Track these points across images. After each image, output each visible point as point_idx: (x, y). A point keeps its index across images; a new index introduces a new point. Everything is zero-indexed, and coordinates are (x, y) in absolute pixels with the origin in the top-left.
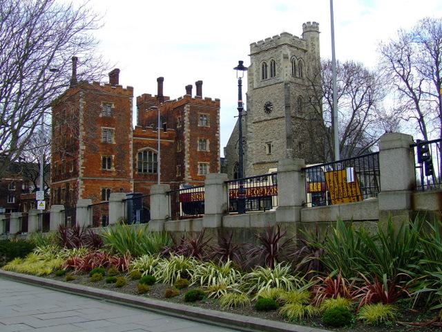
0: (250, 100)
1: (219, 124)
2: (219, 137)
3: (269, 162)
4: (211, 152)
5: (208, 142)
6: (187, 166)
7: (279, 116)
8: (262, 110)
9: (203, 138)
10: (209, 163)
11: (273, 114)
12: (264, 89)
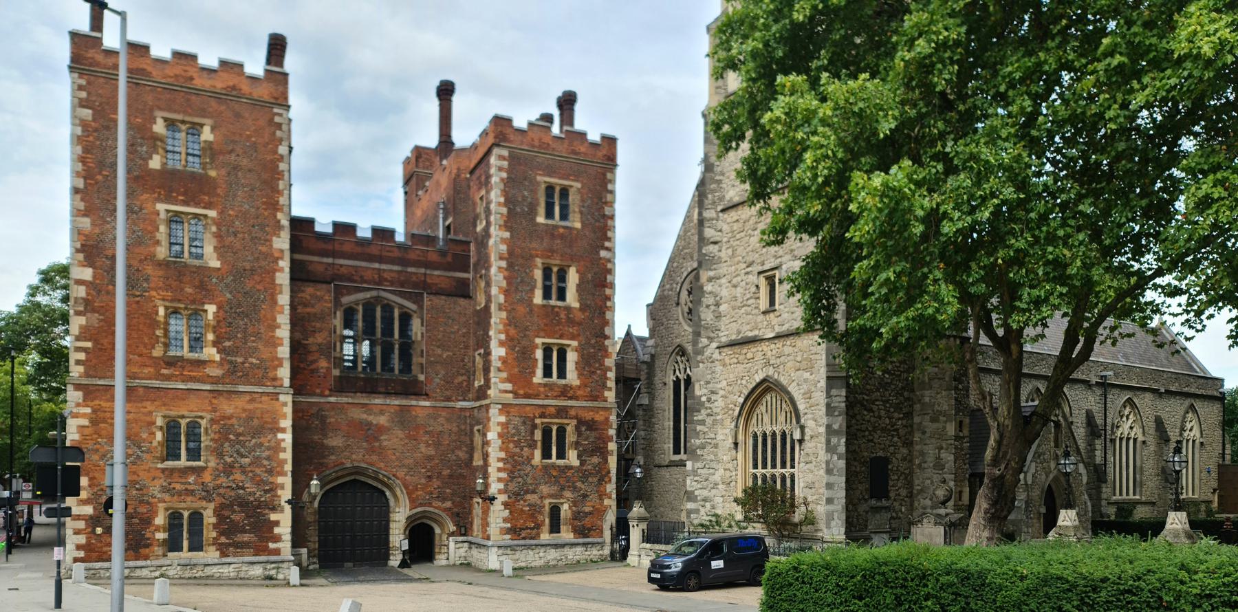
1: (612, 217)
4: (580, 309)
5: (573, 278)
6: (498, 352)
9: (555, 262)
10: (575, 343)
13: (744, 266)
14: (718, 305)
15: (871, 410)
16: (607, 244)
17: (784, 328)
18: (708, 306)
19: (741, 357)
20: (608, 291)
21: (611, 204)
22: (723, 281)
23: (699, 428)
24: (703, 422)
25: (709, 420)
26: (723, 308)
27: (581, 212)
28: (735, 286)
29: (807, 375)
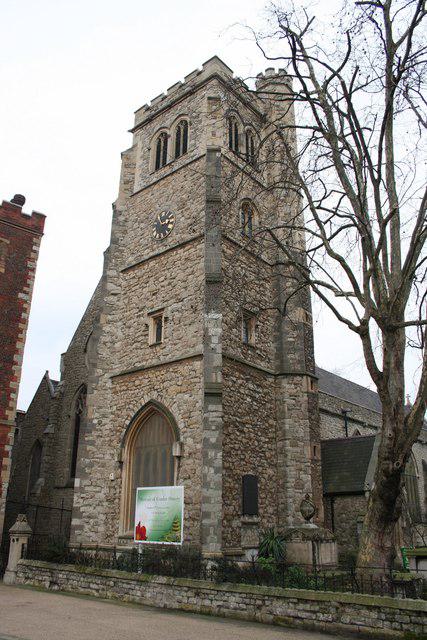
0: (121, 218)
1: (33, 270)
2: (28, 302)
14: (113, 343)
15: (242, 432)
16: (25, 289)
18: (105, 343)
19: (131, 384)
20: (21, 326)
21: (35, 260)
22: (120, 323)
23: (89, 448)
24: (92, 443)
25: (99, 442)
26: (117, 345)
27: (6, 261)
29: (186, 396)
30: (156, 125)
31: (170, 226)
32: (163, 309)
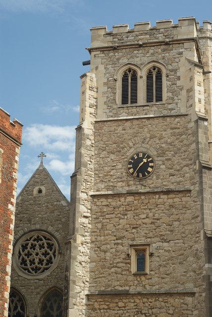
3: (139, 294)
7: (172, 187)
8: (121, 169)
11: (153, 183)
12: (128, 124)
13: (115, 238)
17: (155, 289)
19: (111, 305)
28: (105, 252)
30: (124, 59)
31: (150, 169)
32: (149, 245)
